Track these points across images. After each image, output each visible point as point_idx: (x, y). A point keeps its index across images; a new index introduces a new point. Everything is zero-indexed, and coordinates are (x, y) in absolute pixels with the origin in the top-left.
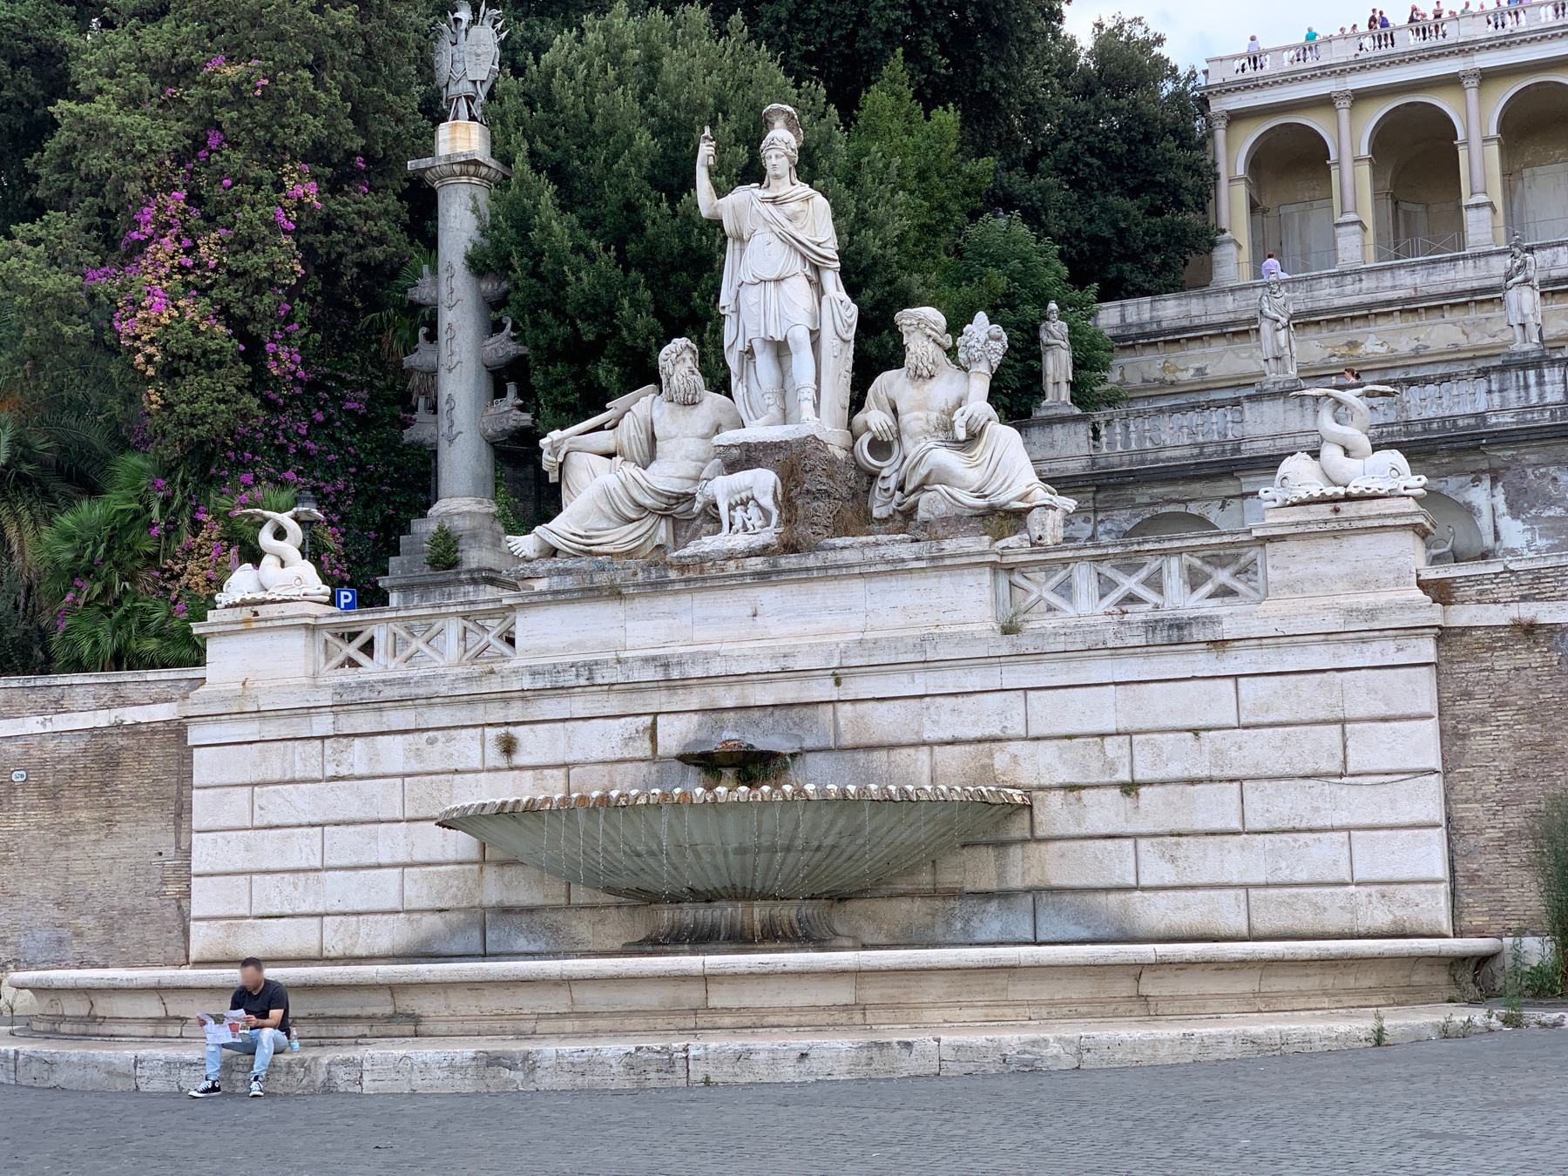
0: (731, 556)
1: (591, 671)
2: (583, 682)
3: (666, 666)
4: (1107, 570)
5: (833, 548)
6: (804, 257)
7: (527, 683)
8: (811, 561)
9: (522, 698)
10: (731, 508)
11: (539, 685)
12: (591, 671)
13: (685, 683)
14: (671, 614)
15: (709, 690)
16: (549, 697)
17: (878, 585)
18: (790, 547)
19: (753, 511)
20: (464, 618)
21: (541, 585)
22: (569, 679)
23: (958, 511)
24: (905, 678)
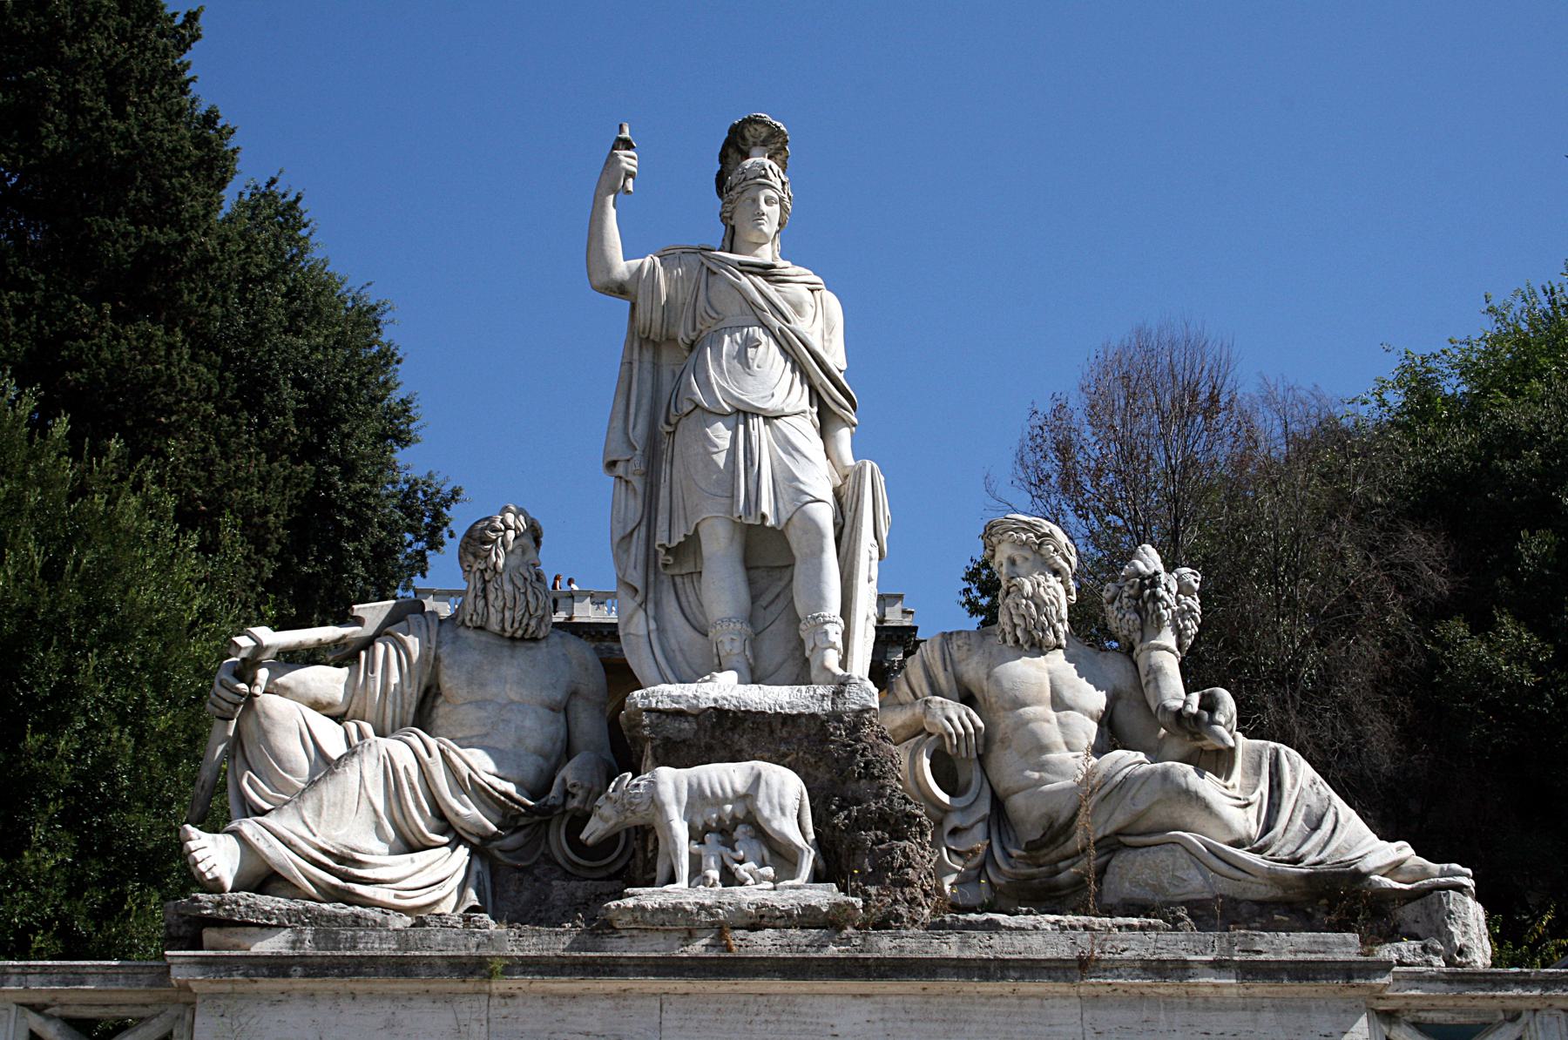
0: (760, 919)
5: (993, 926)
6: (812, 389)
10: (696, 835)
20: (37, 1009)
21: (272, 945)
23: (1225, 887)
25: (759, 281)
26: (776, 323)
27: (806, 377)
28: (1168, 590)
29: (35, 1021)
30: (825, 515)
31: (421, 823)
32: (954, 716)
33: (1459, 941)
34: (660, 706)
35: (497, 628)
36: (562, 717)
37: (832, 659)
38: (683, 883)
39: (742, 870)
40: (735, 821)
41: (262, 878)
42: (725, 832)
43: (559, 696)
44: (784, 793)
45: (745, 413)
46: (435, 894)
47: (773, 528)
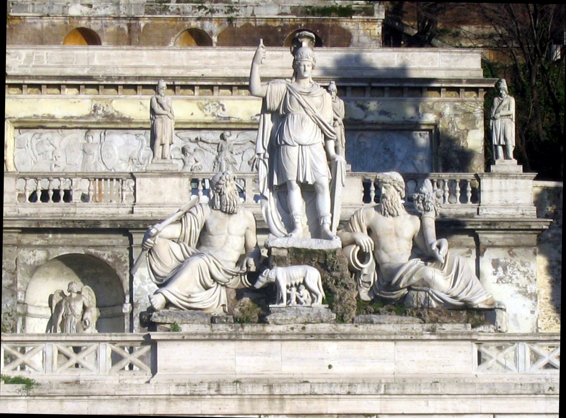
1: (219, 386)
2: (213, 392)
3: (270, 386)
4: (536, 348)
6: (322, 131)
7: (173, 390)
8: (361, 328)
9: (167, 399)
11: (182, 392)
12: (219, 386)
13: (282, 397)
14: (268, 354)
15: (296, 402)
16: (187, 400)
17: (402, 346)
18: (341, 319)
19: (304, 292)
22: (204, 389)
24: (423, 403)
25: (305, 97)
26: (311, 114)
27: (320, 127)
28: (432, 199)
29: (114, 347)
30: (325, 181)
31: (209, 282)
32: (365, 240)
33: (499, 324)
34: (277, 246)
35: (225, 210)
36: (244, 238)
37: (327, 227)
38: (284, 304)
39: (302, 300)
40: (300, 284)
41: (168, 304)
42: (298, 287)
43: (243, 232)
44: (314, 276)
45: (302, 145)
46: (213, 303)
47: (310, 185)
